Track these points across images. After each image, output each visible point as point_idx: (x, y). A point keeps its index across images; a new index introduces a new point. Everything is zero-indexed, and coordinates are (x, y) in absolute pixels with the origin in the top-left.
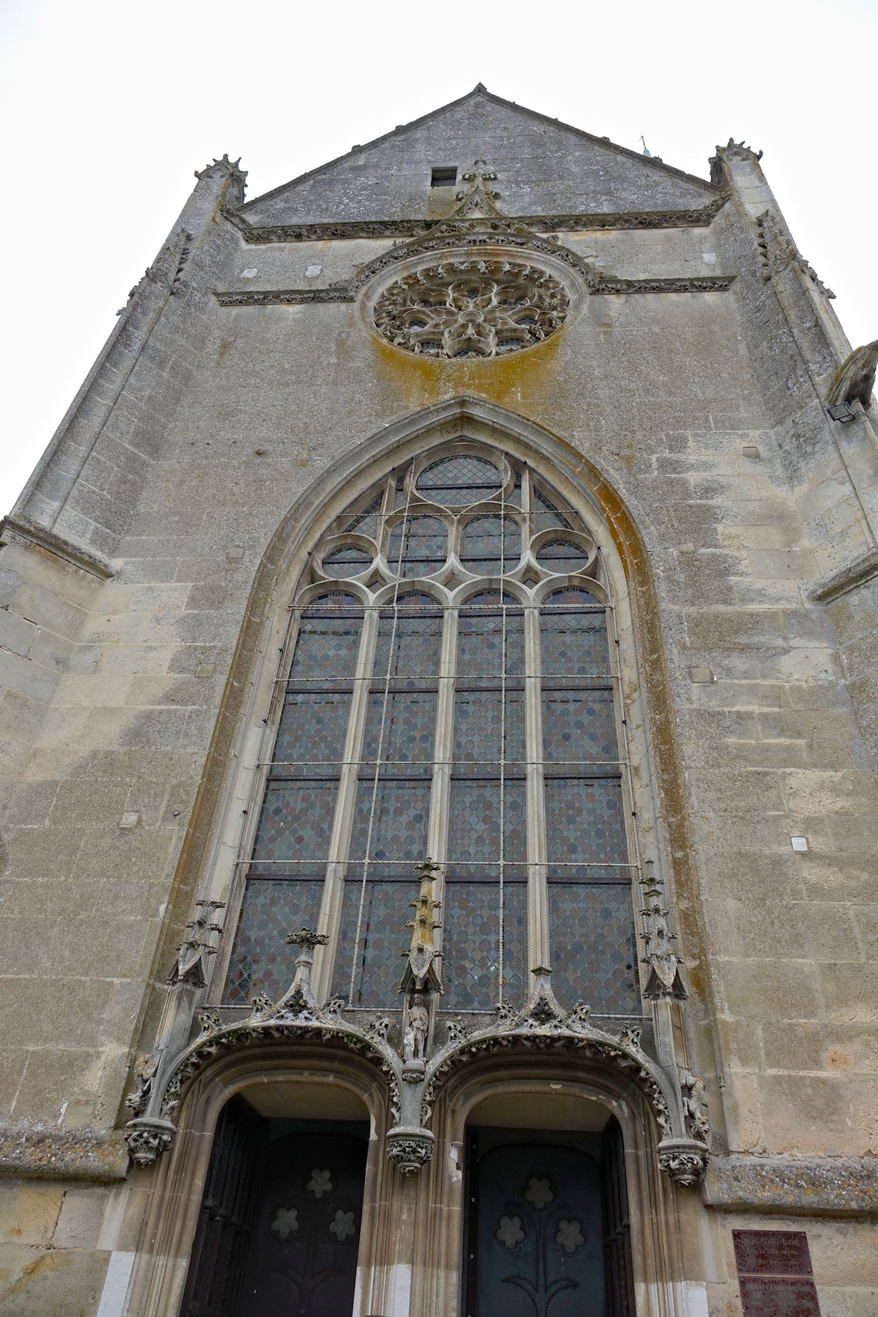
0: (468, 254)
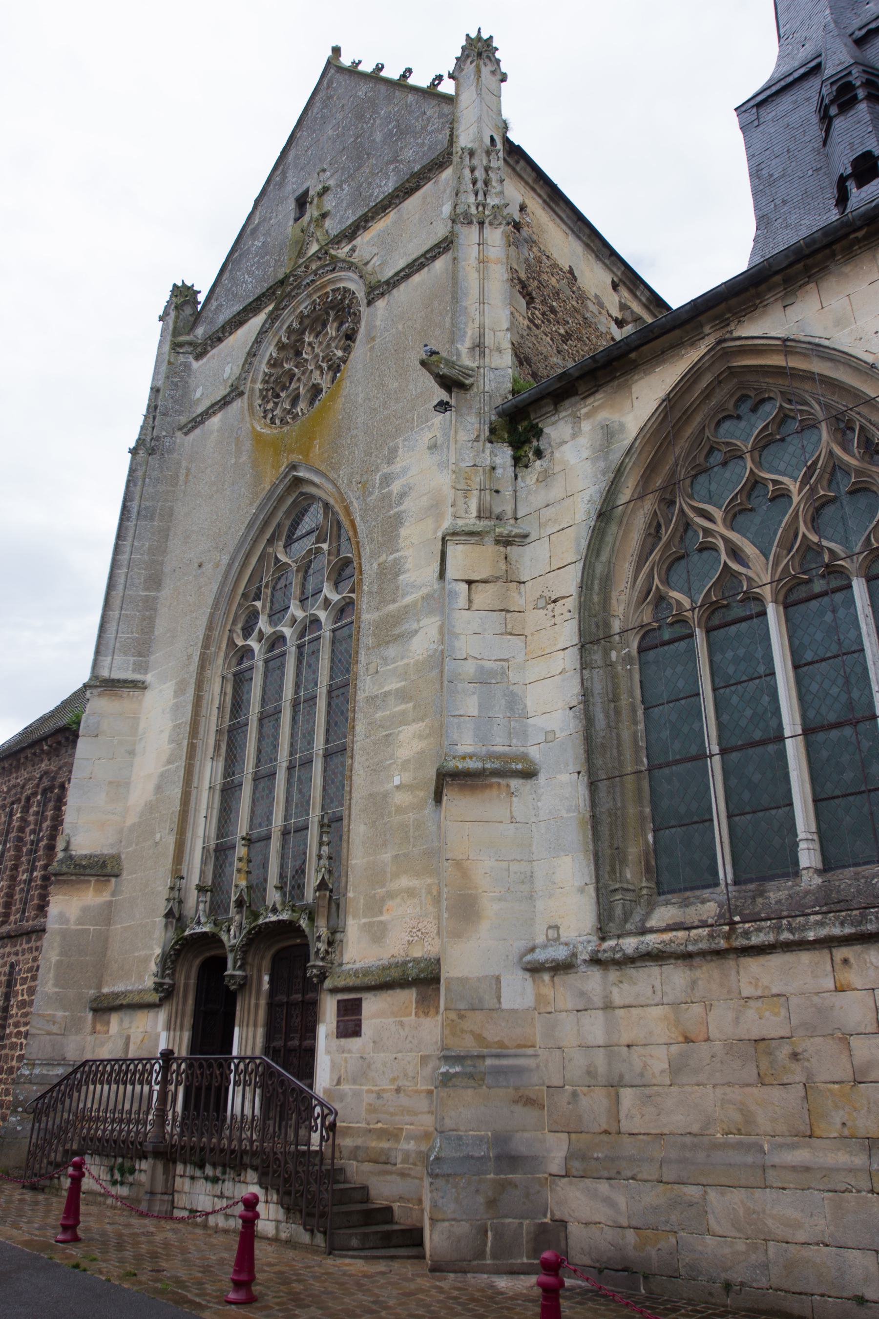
0: (309, 296)
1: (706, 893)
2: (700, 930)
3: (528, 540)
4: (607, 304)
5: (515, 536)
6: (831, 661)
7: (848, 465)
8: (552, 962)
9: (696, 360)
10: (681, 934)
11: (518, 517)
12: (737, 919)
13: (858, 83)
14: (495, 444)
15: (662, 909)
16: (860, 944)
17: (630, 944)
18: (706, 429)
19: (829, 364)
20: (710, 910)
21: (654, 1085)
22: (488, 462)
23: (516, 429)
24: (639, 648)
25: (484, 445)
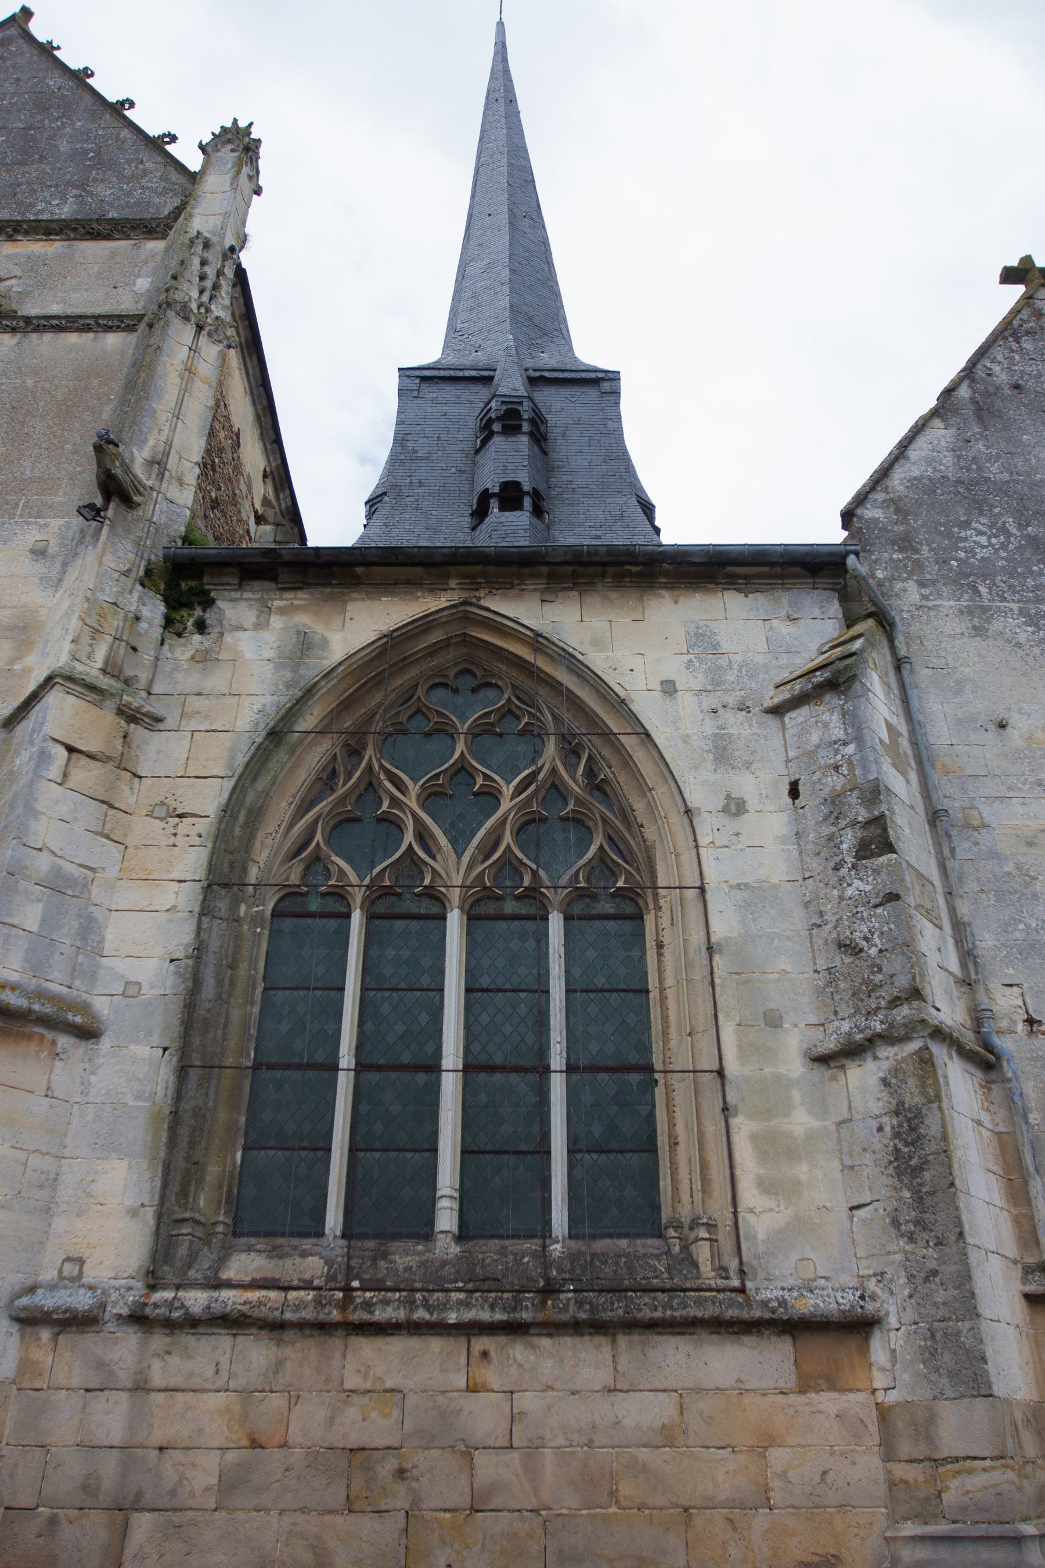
1: (307, 1244)
2: (302, 1293)
3: (161, 726)
4: (254, 490)
5: (146, 715)
6: (509, 994)
7: (571, 791)
8: (65, 1312)
9: (433, 609)
10: (273, 1294)
11: (153, 691)
12: (356, 1284)
13: (526, 417)
14: (146, 590)
15: (243, 1256)
16: (505, 1334)
17: (196, 1300)
18: (419, 687)
19: (575, 679)
20: (314, 1267)
21: (190, 1509)
22: (133, 608)
23: (178, 585)
24: (273, 910)
25: (134, 585)
